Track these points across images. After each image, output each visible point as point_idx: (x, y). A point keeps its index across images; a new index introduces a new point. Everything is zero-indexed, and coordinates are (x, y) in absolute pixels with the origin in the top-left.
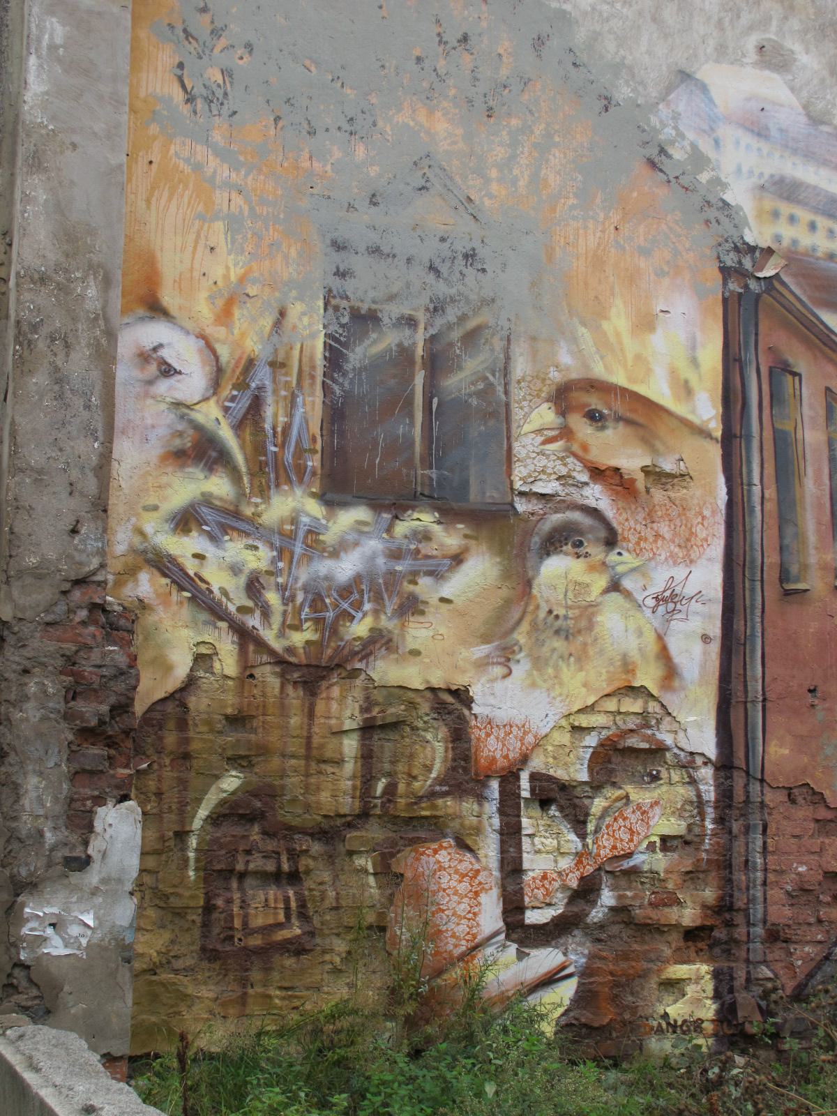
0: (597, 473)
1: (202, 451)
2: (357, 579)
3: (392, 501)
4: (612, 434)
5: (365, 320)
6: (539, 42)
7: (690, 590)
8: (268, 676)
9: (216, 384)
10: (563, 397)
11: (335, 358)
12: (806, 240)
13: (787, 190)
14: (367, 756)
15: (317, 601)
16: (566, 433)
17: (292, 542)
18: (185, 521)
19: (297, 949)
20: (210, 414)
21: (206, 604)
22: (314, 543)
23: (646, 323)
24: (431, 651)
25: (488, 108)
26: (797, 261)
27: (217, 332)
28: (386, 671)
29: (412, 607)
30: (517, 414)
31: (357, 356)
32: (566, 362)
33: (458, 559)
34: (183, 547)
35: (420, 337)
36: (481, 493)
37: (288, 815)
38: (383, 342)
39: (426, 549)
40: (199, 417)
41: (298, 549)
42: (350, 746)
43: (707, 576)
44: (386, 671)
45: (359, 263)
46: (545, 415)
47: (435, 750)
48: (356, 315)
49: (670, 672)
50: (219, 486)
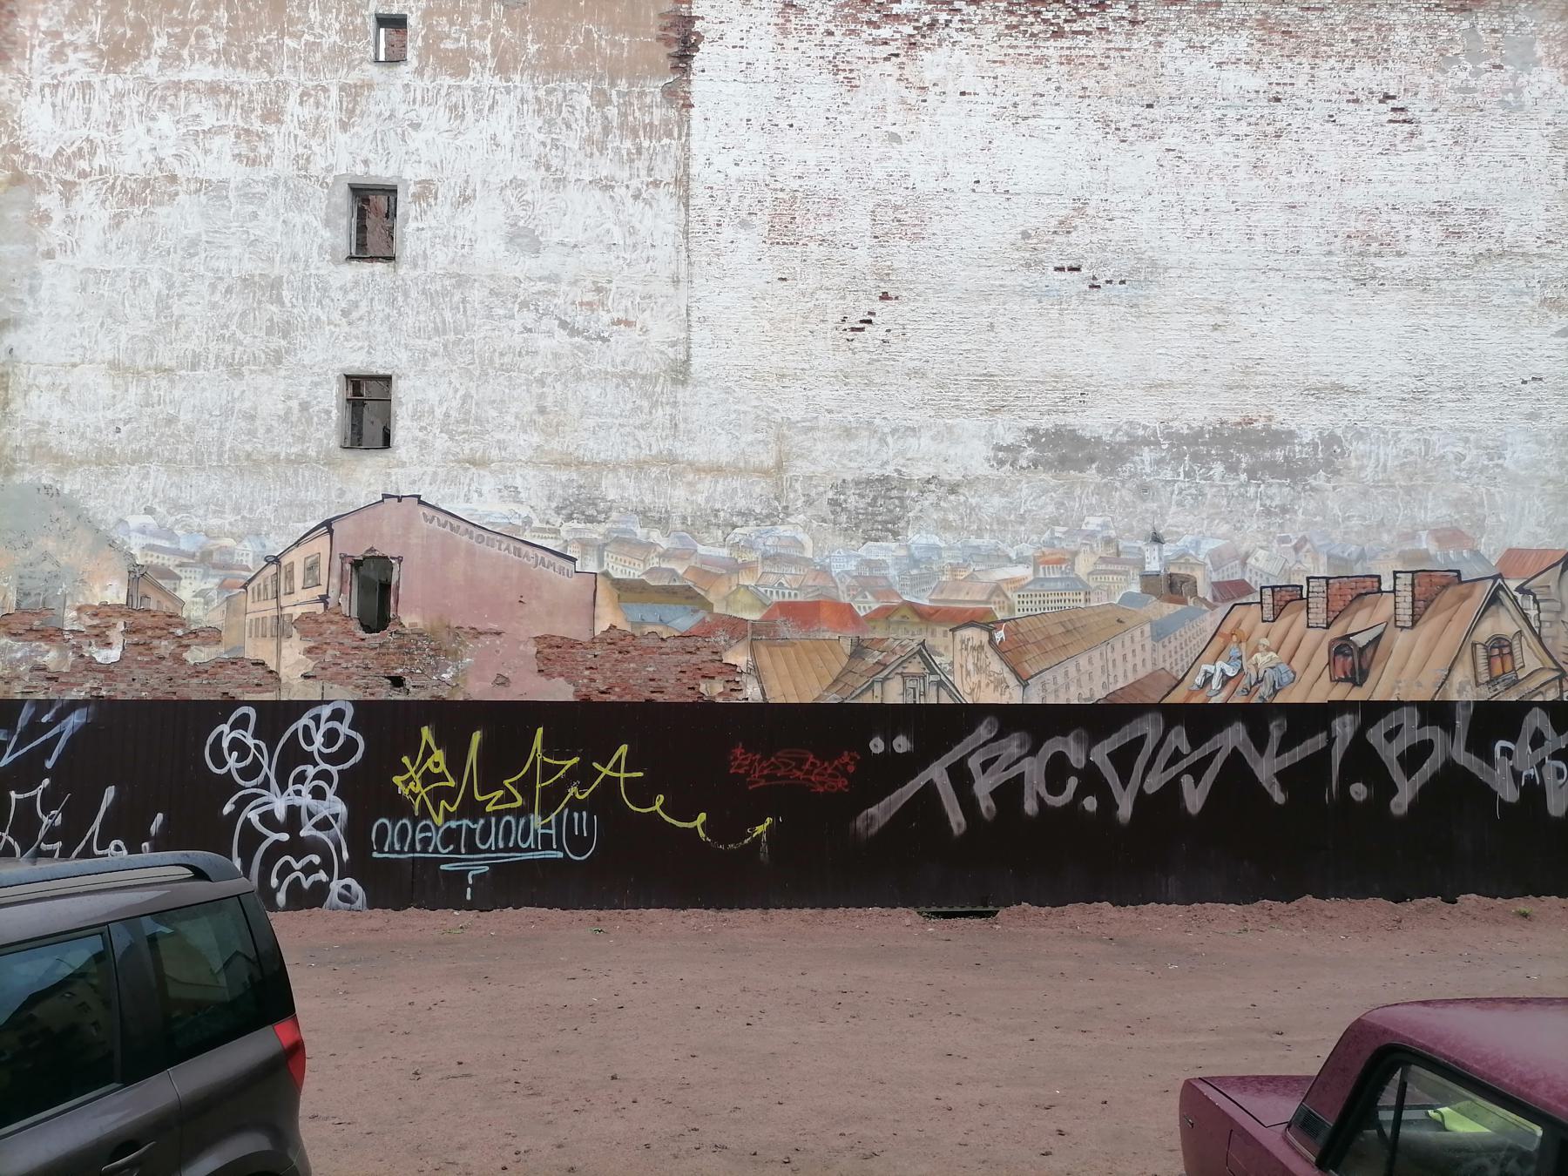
10: (79, 609)
16: (79, 618)
32: (81, 601)
46: (74, 614)
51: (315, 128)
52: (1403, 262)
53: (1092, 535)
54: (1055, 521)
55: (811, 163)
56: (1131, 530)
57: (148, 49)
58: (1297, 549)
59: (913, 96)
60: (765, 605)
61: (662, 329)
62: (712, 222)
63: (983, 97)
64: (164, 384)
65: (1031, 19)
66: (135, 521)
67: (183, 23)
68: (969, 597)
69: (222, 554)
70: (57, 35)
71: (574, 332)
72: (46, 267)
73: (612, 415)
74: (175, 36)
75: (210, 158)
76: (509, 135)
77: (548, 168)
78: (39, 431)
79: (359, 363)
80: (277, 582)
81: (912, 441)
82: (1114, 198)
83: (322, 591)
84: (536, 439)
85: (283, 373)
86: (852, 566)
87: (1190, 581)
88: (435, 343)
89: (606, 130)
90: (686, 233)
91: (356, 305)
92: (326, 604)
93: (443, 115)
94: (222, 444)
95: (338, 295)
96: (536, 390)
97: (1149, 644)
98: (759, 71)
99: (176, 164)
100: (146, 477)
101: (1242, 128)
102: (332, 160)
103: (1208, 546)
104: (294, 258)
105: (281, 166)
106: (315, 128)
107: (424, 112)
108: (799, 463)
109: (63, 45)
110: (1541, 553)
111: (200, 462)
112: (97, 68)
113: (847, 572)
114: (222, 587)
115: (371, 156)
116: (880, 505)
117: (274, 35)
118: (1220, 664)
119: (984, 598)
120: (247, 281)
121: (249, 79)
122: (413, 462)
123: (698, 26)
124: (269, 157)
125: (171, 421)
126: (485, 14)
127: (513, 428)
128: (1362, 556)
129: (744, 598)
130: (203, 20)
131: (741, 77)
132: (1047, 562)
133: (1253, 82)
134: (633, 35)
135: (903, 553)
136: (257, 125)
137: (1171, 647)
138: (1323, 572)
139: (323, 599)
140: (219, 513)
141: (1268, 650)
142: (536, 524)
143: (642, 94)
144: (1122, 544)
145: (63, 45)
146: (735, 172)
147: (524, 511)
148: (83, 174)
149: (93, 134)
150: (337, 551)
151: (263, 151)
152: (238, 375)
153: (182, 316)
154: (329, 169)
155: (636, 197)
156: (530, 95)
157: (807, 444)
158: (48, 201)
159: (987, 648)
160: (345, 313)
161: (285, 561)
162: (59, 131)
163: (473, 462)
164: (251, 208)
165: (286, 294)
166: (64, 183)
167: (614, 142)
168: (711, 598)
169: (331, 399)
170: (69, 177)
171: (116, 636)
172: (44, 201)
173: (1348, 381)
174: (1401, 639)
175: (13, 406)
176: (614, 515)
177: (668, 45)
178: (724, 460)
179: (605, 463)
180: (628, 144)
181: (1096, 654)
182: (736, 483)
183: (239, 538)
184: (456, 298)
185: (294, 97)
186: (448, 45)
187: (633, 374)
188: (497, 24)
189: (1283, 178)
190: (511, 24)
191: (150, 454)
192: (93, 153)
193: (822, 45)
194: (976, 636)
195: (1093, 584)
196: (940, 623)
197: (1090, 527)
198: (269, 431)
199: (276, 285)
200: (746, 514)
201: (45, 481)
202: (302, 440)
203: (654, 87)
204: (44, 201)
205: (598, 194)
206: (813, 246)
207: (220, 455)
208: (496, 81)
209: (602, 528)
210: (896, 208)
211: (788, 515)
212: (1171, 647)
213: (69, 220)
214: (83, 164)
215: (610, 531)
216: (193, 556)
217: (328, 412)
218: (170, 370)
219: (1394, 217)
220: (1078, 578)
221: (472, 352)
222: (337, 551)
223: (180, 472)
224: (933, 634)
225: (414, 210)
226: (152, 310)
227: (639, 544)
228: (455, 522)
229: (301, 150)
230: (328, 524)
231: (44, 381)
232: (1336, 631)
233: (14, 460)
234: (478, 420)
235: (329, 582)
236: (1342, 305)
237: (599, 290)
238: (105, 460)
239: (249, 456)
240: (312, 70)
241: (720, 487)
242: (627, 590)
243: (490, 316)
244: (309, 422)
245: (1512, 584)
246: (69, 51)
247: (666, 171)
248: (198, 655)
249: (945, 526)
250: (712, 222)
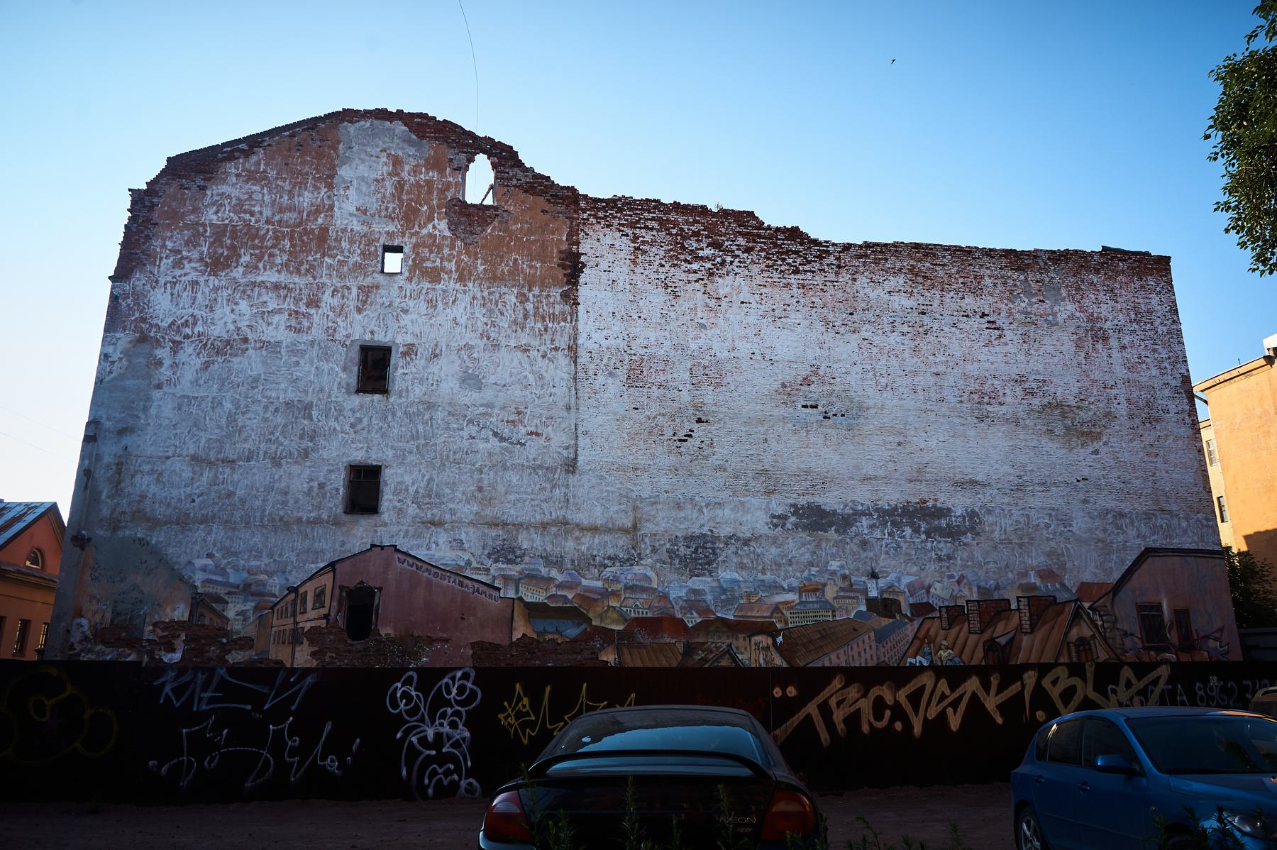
5: (119, 614)
10: (155, 625)
16: (154, 631)
22: (104, 654)
26: (208, 595)
51: (341, 311)
52: (1004, 408)
53: (834, 573)
55: (652, 339)
56: (858, 570)
57: (237, 262)
58: (959, 582)
59: (712, 303)
60: (626, 620)
61: (559, 438)
62: (591, 373)
63: (754, 305)
64: (228, 470)
65: (779, 262)
66: (199, 563)
67: (261, 248)
68: (759, 614)
70: (179, 252)
71: (502, 439)
72: (157, 394)
73: (526, 493)
74: (256, 255)
75: (271, 328)
76: (464, 318)
77: (488, 338)
78: (139, 501)
79: (358, 456)
81: (719, 512)
82: (835, 366)
83: (324, 611)
84: (475, 508)
85: (308, 464)
86: (683, 593)
87: (897, 603)
88: (412, 445)
89: (526, 317)
90: (575, 379)
91: (360, 420)
92: (328, 621)
93: (423, 306)
94: (264, 511)
95: (350, 414)
96: (476, 476)
97: (874, 645)
98: (620, 285)
99: (248, 331)
100: (209, 533)
101: (905, 328)
102: (350, 331)
103: (906, 580)
104: (322, 390)
105: (317, 333)
106: (341, 311)
107: (411, 303)
108: (648, 525)
109: (182, 258)
110: (1100, 585)
111: (248, 523)
112: (203, 272)
114: (256, 608)
115: (376, 329)
116: (700, 553)
117: (318, 256)
118: (919, 658)
120: (289, 405)
121: (301, 281)
122: (393, 524)
123: (583, 259)
124: (309, 328)
125: (230, 495)
126: (452, 247)
127: (461, 501)
128: (997, 587)
130: (274, 246)
131: (609, 288)
132: (807, 591)
133: (910, 303)
134: (543, 262)
135: (715, 584)
136: (303, 309)
137: (888, 647)
138: (975, 597)
139: (326, 617)
140: (258, 557)
141: (947, 648)
142: (474, 565)
143: (548, 296)
144: (853, 579)
145: (182, 258)
146: (605, 343)
147: (466, 556)
148: (187, 337)
149: (196, 312)
150: (338, 583)
151: (306, 324)
152: (279, 465)
153: (244, 427)
154: (348, 336)
155: (543, 357)
156: (479, 295)
157: (653, 513)
158: (163, 353)
160: (352, 426)
161: (302, 590)
162: (174, 310)
163: (433, 523)
164: (295, 359)
165: (315, 413)
166: (174, 342)
167: (530, 323)
168: (591, 615)
169: (339, 481)
170: (177, 338)
171: (179, 644)
172: (159, 353)
173: (980, 478)
174: (1026, 640)
175: (123, 485)
176: (527, 559)
177: (564, 269)
178: (599, 523)
179: (521, 524)
180: (539, 325)
181: (841, 652)
182: (607, 538)
183: (271, 574)
184: (426, 417)
185: (328, 292)
186: (428, 264)
187: (540, 467)
188: (460, 253)
189: (931, 358)
190: (468, 253)
191: (214, 516)
192: (195, 324)
193: (657, 272)
194: (763, 640)
195: (837, 606)
196: (741, 632)
197: (833, 568)
198: (296, 502)
199: (308, 407)
200: (613, 559)
201: (139, 535)
203: (556, 293)
204: (159, 353)
205: (520, 354)
206: (654, 388)
207: (262, 518)
208: (457, 286)
209: (518, 568)
210: (705, 367)
211: (641, 559)
212: (888, 647)
213: (175, 365)
214: (188, 331)
215: (523, 569)
216: (238, 587)
217: (337, 490)
218: (233, 461)
219: (996, 382)
220: (827, 601)
222: (338, 583)
223: (233, 529)
224: (737, 639)
225: (401, 362)
226: (224, 421)
227: (543, 578)
228: (419, 564)
229: (330, 324)
230: (332, 566)
231: (146, 468)
232: (987, 636)
234: (438, 495)
236: (971, 433)
237: (519, 413)
238: (183, 522)
239: (281, 519)
240: (341, 276)
241: (596, 540)
242: (534, 610)
243: (448, 429)
244: (324, 496)
245: (1086, 605)
246: (185, 262)
247: (563, 342)
248: (236, 657)
249: (742, 566)
250: (591, 373)
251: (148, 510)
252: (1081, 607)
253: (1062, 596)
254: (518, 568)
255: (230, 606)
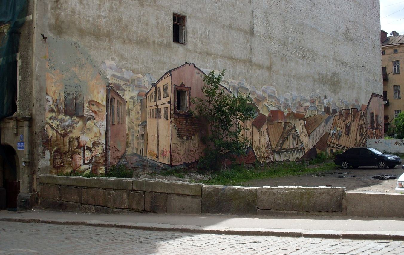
0: (93, 111)
1: (52, 111)
2: (68, 125)
3: (72, 115)
4: (95, 107)
5: (69, 94)
6: (87, 59)
7: (102, 125)
8: (59, 136)
9: (53, 103)
11: (65, 99)
12: (116, 82)
13: (114, 76)
14: (69, 144)
15: (64, 127)
16: (90, 107)
17: (62, 121)
18: (51, 119)
19: (63, 166)
20: (53, 106)
21: (53, 128)
23: (98, 93)
24: (76, 133)
25: (81, 67)
26: (115, 84)
27: (53, 96)
28: (71, 135)
29: (74, 128)
30: (84, 105)
31: (68, 99)
32: (90, 98)
33: (78, 122)
34: (50, 122)
35: (74, 96)
36: (81, 114)
37: (61, 151)
38: (70, 97)
39: (75, 121)
40: (52, 107)
41: (62, 121)
42: (68, 143)
43: (104, 123)
44: (71, 135)
45: (68, 87)
47: (76, 143)
48: (68, 94)
49: (100, 134)
50: (54, 114)
53: (317, 95)
54: (313, 91)
66: (109, 63)
69: (138, 81)
78: (71, 16)
79: (177, 9)
80: (156, 93)
83: (168, 99)
97: (325, 125)
103: (332, 100)
113: (283, 102)
114: (139, 95)
119: (303, 111)
129: (265, 109)
139: (170, 102)
144: (322, 98)
159: (304, 126)
161: (158, 86)
169: (170, 23)
173: (346, 61)
174: (352, 124)
183: (144, 74)
194: (302, 121)
198: (152, 31)
201: (74, 40)
202: (162, 36)
212: (328, 125)
215: (239, 83)
216: (129, 81)
217: (169, 27)
221: (207, 13)
230: (170, 71)
232: (346, 123)
233: (61, 28)
235: (172, 97)
245: (363, 112)
251: (77, 22)
252: (361, 113)
253: (359, 109)
254: (237, 82)
255: (126, 92)
